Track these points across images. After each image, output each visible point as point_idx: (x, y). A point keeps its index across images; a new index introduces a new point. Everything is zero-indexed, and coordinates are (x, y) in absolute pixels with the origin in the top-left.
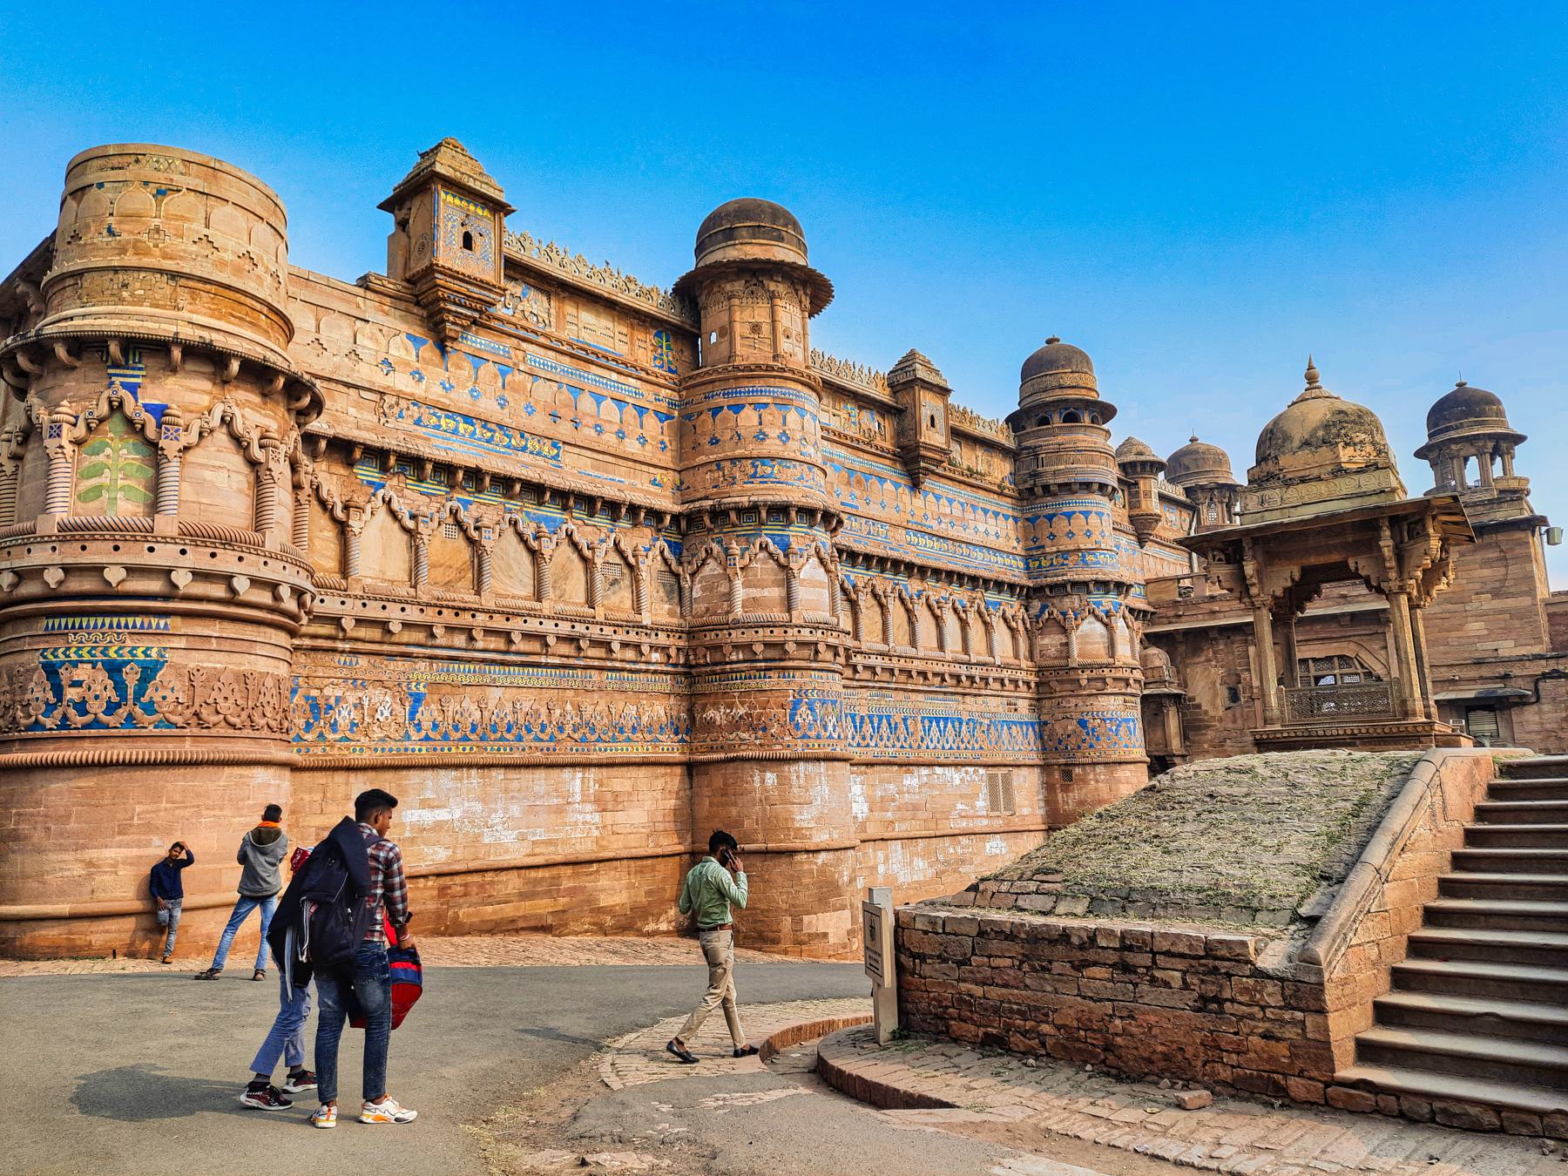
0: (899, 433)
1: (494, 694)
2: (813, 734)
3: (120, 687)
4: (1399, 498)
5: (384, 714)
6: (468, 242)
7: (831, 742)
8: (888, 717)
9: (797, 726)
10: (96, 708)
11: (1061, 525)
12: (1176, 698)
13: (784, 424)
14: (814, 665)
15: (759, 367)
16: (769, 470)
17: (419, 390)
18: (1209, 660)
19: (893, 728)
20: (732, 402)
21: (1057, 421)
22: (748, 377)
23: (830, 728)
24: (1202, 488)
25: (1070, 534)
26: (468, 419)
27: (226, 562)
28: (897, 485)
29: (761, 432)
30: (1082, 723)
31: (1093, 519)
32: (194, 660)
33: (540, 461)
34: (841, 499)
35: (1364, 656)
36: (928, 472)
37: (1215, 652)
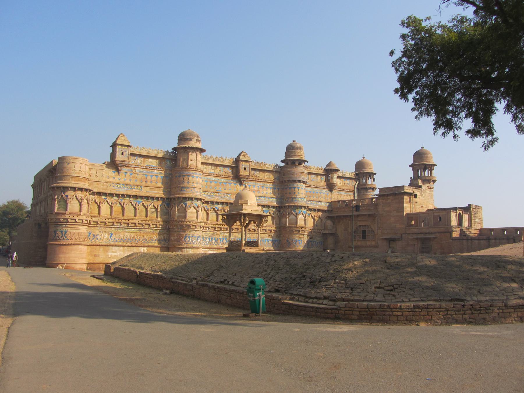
1: (126, 234)
3: (62, 234)
5: (106, 237)
6: (123, 154)
10: (60, 237)
11: (288, 191)
12: (332, 234)
17: (114, 181)
26: (123, 184)
27: (75, 217)
30: (287, 241)
31: (300, 189)
32: (71, 231)
33: (138, 190)
36: (244, 181)
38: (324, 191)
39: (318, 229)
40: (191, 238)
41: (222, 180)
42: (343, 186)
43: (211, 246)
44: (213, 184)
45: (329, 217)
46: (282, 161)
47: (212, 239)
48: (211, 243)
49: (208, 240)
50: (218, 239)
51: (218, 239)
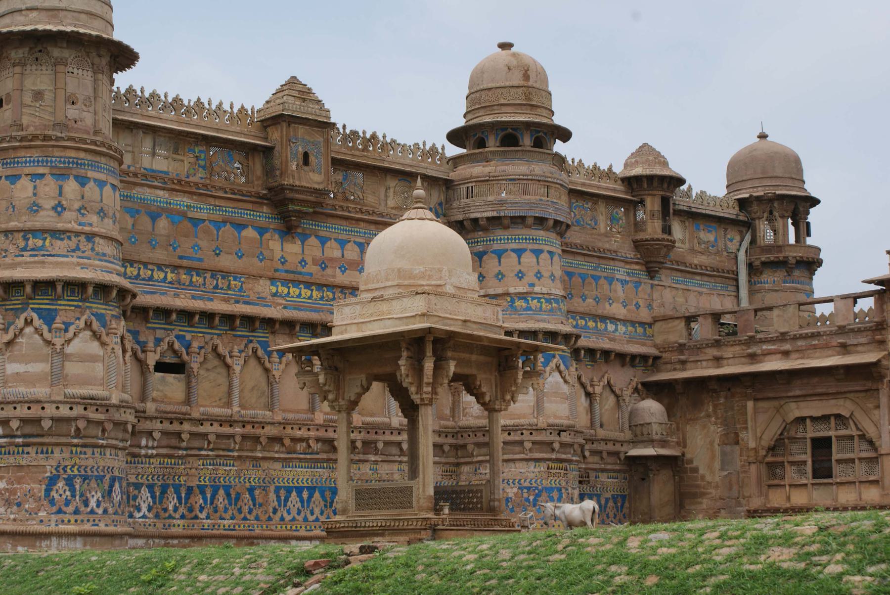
0: (269, 171)
2: (71, 509)
4: (335, 337)
7: (91, 517)
8: (227, 489)
9: (52, 502)
13: (60, 194)
14: (75, 441)
15: (35, 137)
16: (40, 243)
18: (709, 416)
19: (234, 499)
20: (9, 173)
21: (492, 144)
22: (25, 147)
23: (93, 503)
24: (758, 198)
25: (500, 276)
28: (262, 231)
29: (35, 204)
34: (179, 252)
35: (859, 415)
36: (301, 215)
37: (715, 407)
38: (621, 273)
39: (606, 441)
40: (78, 482)
41: (203, 210)
42: (692, 251)
43: (159, 528)
44: (163, 224)
45: (644, 384)
46: (455, 137)
47: (164, 489)
48: (159, 510)
49: (145, 493)
50: (190, 490)
51: (190, 490)
